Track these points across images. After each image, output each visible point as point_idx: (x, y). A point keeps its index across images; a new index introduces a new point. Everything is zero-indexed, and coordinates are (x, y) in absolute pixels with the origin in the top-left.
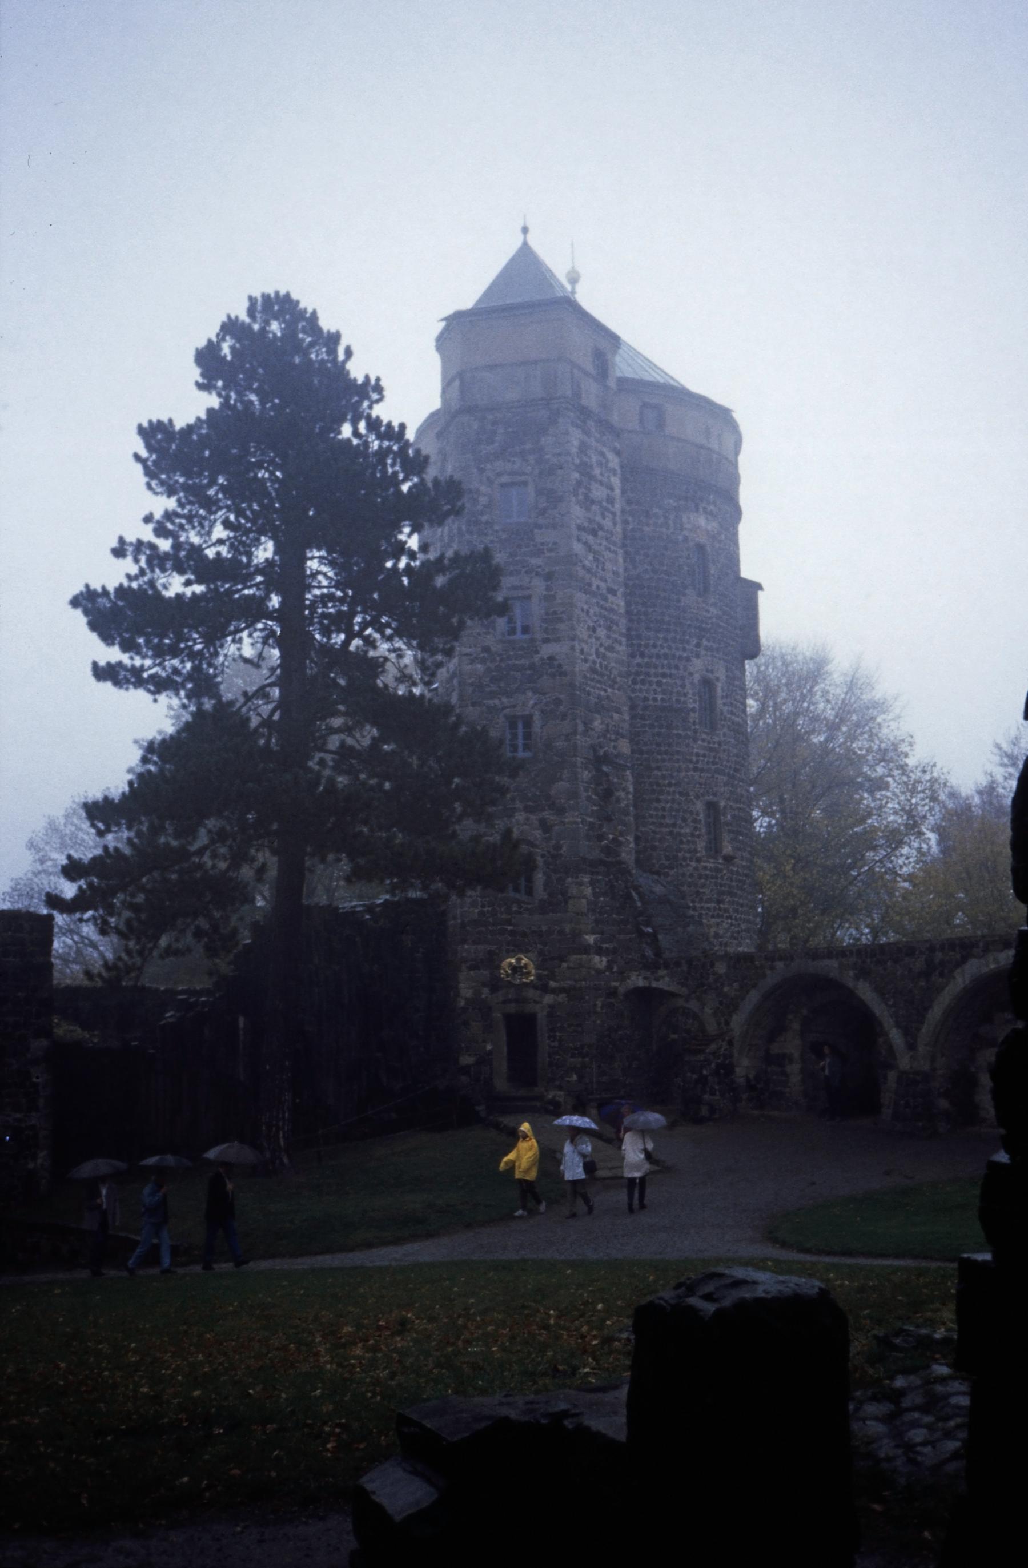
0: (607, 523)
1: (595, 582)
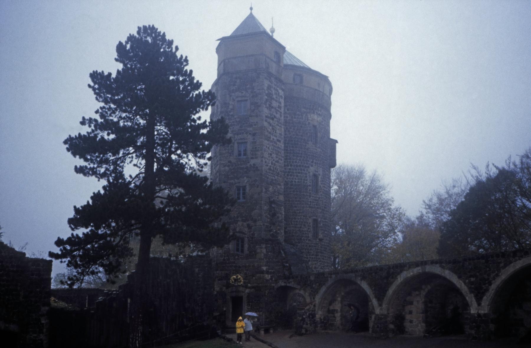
0: (278, 116)
1: (272, 137)
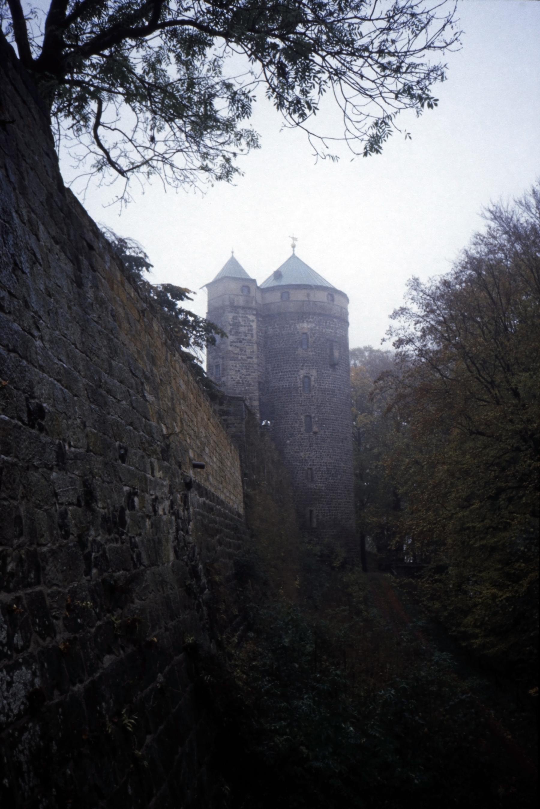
1: (240, 357)
